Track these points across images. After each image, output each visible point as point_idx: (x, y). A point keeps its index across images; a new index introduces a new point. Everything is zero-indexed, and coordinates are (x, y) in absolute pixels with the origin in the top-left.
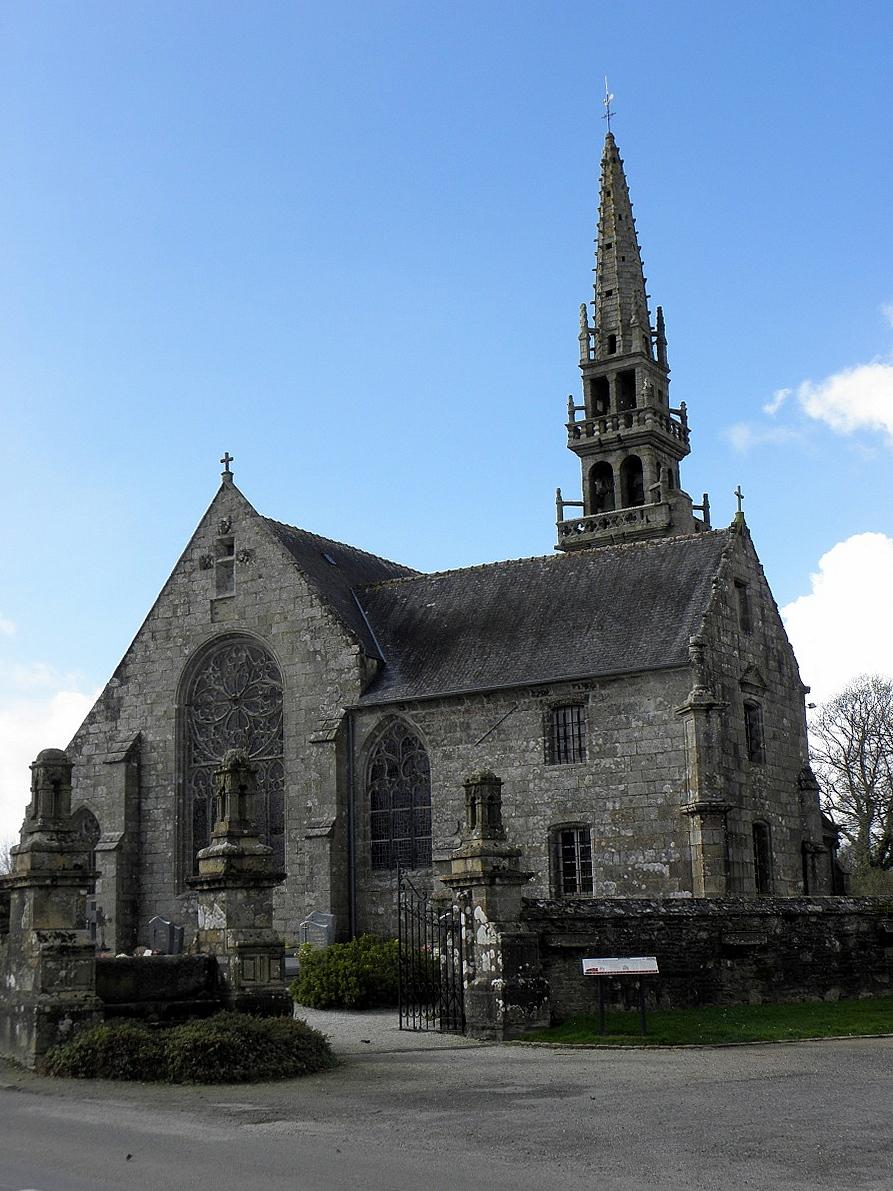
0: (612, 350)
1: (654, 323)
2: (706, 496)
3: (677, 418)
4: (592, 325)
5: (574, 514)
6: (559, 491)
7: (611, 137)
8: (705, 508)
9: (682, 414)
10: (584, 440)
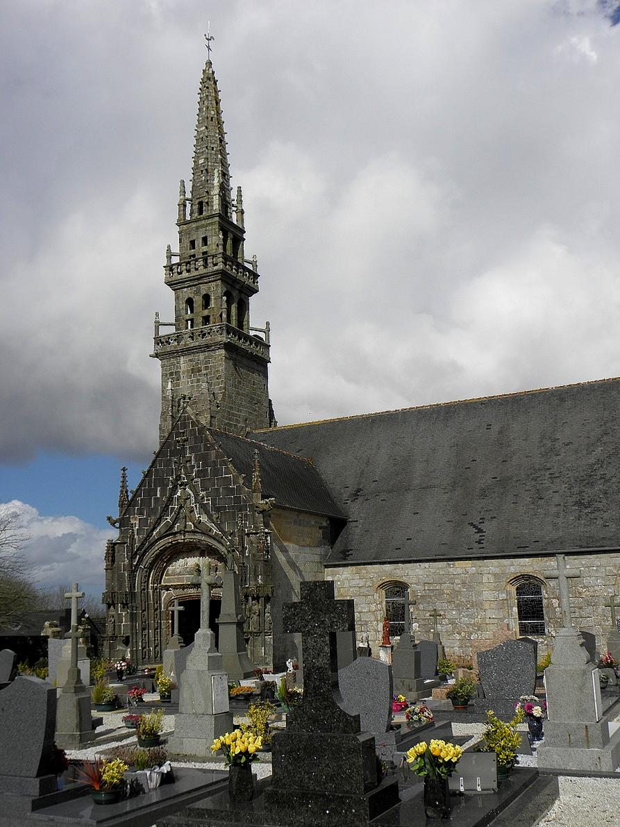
0: (201, 212)
1: (234, 195)
2: (268, 324)
3: (250, 267)
4: (189, 195)
5: (164, 331)
6: (157, 314)
7: (209, 64)
8: (267, 331)
9: (254, 263)
10: (176, 277)
